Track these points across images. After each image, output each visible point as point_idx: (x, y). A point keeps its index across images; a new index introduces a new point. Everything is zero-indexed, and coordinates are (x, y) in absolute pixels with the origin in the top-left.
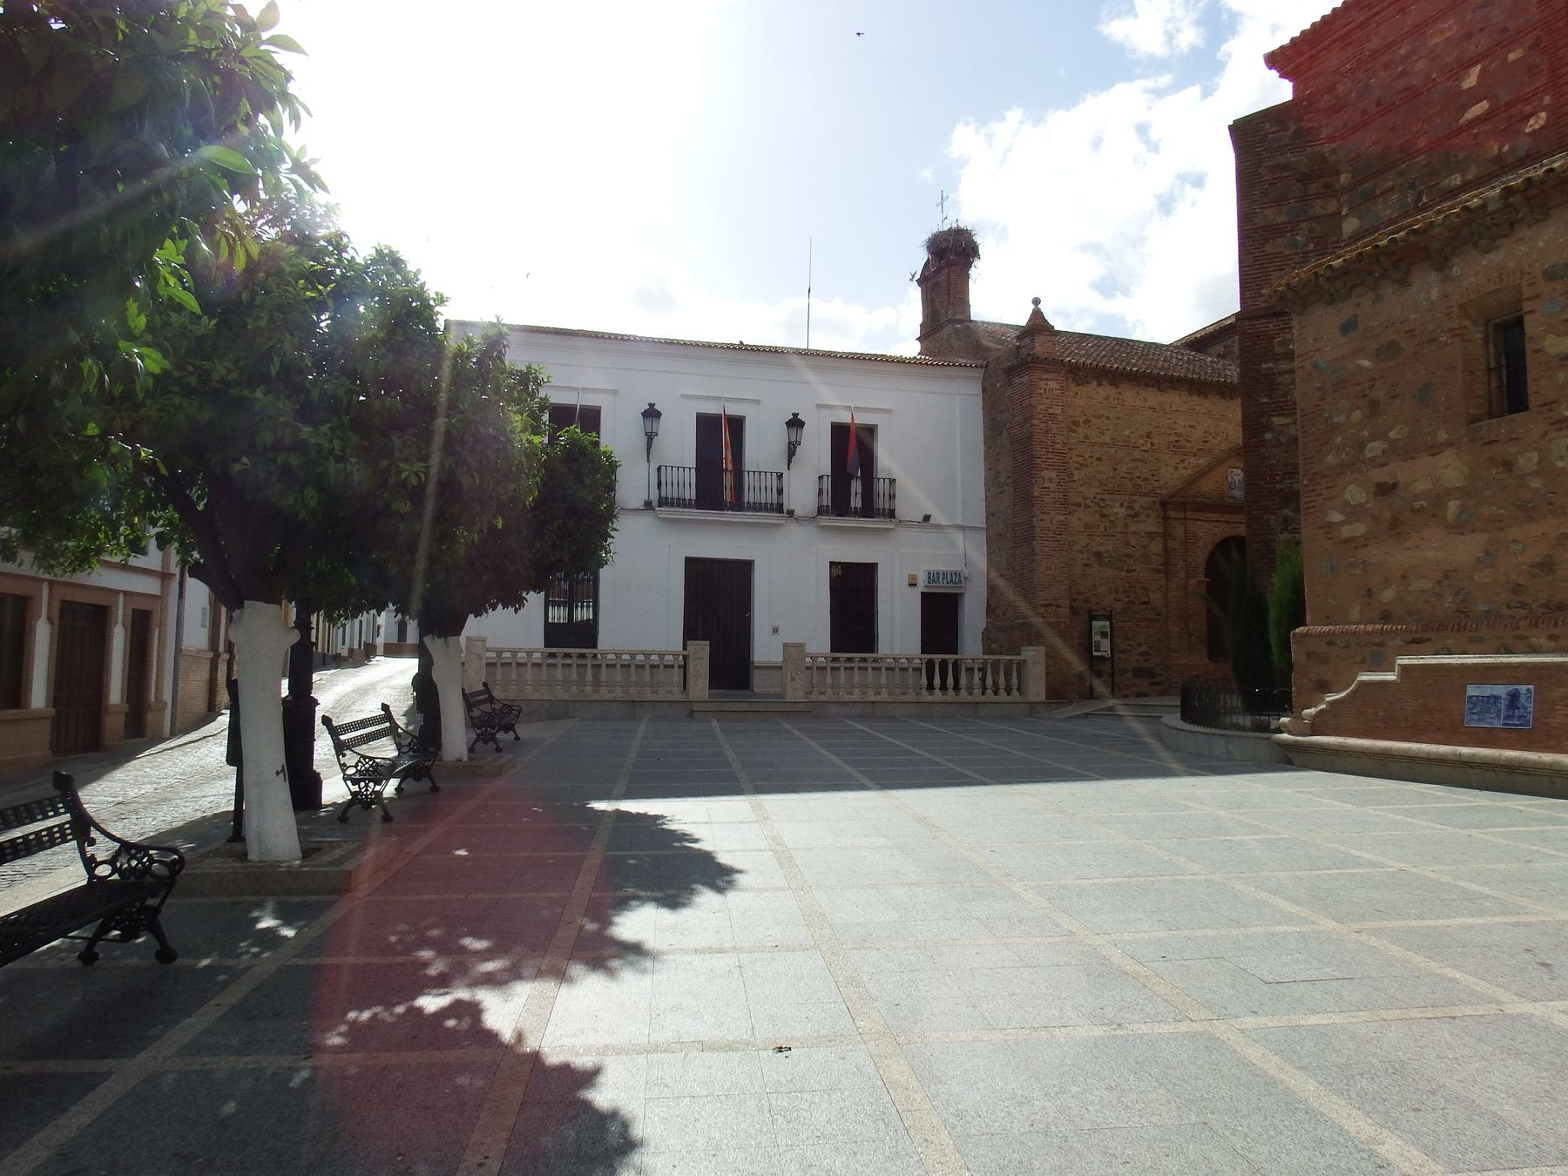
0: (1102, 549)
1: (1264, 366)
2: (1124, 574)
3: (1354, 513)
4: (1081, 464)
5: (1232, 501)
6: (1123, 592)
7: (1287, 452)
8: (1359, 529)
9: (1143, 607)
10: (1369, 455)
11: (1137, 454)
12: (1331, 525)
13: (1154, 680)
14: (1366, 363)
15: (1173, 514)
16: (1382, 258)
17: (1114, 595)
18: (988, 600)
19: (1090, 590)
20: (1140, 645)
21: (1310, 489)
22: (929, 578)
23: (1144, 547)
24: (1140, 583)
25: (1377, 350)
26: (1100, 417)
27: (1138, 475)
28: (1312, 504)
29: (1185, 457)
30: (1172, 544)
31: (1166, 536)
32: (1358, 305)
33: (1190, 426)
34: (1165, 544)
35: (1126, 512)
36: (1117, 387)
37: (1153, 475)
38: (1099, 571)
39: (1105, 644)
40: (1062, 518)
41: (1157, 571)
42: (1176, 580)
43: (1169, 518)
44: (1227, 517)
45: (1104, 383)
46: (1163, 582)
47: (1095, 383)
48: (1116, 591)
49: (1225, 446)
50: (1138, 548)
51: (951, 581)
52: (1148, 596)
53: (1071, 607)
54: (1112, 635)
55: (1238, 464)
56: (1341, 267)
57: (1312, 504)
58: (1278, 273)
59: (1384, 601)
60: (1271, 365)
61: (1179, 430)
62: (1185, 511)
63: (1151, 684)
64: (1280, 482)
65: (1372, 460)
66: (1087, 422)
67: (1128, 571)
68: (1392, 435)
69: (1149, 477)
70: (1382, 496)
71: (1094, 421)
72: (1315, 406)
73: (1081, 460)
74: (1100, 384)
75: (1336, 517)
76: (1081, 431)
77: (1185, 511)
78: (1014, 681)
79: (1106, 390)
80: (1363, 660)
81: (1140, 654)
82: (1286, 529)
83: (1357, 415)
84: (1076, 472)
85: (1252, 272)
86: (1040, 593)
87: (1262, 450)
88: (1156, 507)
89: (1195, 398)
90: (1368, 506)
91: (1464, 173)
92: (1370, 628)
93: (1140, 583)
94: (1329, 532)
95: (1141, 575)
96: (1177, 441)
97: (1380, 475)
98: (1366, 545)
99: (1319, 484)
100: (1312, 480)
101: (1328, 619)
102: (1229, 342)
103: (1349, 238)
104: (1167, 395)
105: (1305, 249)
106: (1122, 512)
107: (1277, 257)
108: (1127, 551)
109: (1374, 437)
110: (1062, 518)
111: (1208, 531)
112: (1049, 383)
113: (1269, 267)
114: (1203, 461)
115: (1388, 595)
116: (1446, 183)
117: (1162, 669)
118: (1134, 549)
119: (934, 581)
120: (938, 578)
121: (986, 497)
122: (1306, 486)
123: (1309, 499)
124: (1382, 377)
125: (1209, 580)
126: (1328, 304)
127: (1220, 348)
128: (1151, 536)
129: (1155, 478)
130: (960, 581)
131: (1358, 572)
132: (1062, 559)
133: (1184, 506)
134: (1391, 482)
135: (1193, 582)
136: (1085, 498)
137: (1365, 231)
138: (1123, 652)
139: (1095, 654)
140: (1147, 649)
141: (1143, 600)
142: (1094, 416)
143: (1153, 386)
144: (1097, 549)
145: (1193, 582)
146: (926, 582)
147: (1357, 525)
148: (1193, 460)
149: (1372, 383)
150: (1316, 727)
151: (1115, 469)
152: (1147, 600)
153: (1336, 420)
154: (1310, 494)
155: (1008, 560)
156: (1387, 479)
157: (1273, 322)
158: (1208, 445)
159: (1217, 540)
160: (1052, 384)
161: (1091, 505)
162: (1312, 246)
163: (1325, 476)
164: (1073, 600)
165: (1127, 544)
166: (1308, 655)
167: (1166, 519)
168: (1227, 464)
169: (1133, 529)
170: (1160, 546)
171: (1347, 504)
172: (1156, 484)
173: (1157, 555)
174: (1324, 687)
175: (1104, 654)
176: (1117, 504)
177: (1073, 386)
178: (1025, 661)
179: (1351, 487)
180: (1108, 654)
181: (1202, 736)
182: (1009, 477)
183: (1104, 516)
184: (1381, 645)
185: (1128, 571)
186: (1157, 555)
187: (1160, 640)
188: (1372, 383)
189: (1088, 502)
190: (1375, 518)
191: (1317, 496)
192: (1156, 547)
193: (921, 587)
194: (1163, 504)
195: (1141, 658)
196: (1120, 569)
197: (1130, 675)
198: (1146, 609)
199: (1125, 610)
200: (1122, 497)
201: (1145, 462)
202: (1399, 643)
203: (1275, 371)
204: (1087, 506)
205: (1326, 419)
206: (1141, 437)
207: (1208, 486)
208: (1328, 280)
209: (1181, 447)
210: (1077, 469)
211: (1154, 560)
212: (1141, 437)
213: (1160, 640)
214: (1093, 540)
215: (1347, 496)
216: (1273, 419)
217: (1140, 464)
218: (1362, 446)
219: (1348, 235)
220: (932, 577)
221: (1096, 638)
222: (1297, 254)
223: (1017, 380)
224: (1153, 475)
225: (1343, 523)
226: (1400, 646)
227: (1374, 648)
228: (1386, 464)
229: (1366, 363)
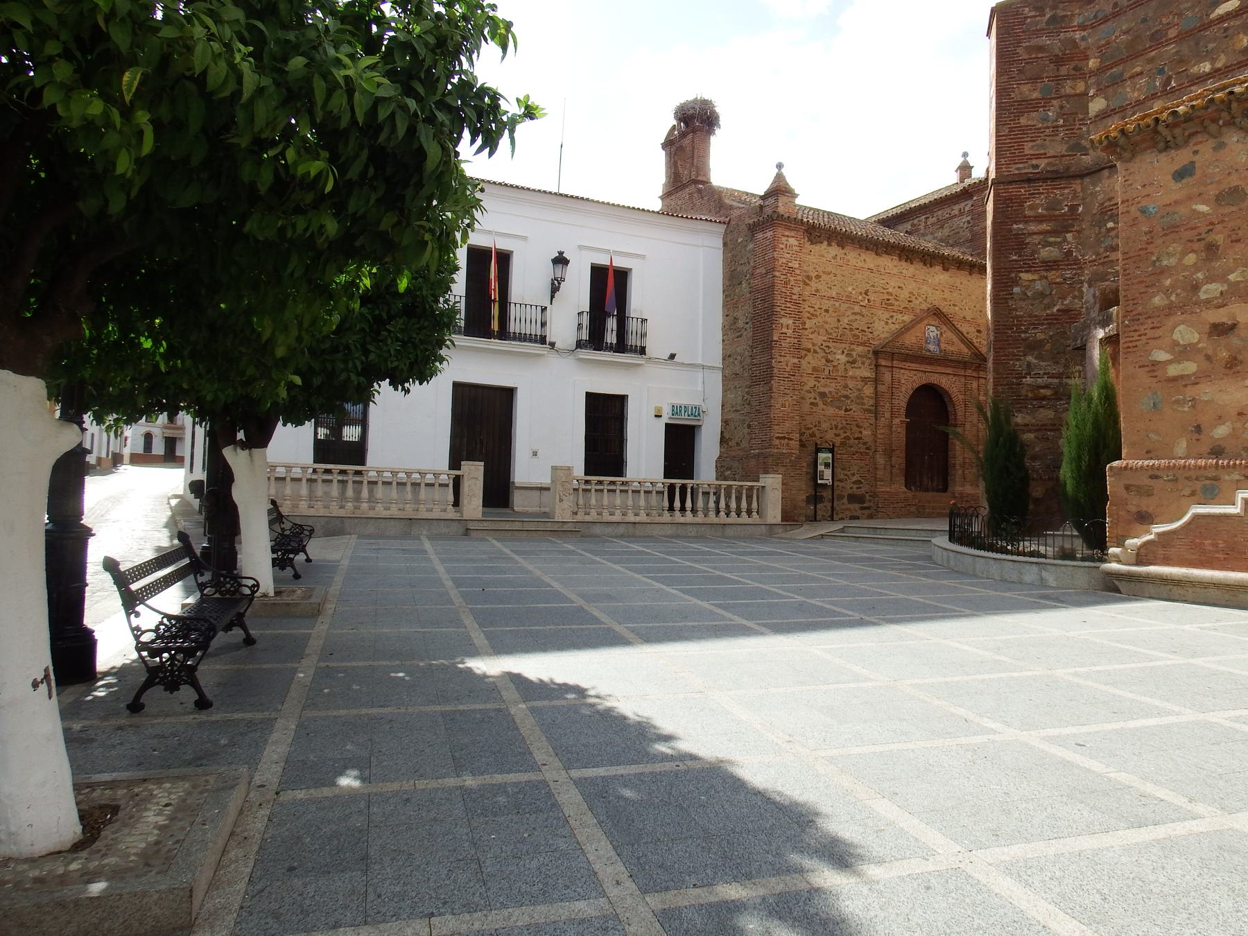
0: (826, 390)
2: (843, 412)
3: (1183, 352)
4: (812, 315)
5: (929, 354)
6: (842, 429)
7: (1032, 305)
8: (1190, 367)
9: (856, 441)
10: (1203, 296)
11: (857, 308)
12: (1155, 364)
13: (865, 505)
14: (1203, 208)
15: (883, 363)
16: (1234, 105)
17: (834, 431)
18: (722, 432)
19: (815, 426)
21: (1132, 329)
22: (673, 410)
23: (859, 390)
25: (1216, 196)
26: (829, 274)
28: (1134, 344)
29: (894, 314)
30: (881, 388)
31: (876, 381)
32: (1196, 152)
33: (899, 287)
34: (876, 387)
35: (847, 359)
36: (843, 248)
38: (823, 410)
39: (828, 473)
40: (796, 361)
41: (868, 411)
42: (883, 419)
43: (880, 365)
45: (833, 244)
46: (873, 421)
47: (825, 243)
48: (836, 427)
49: (925, 306)
51: (677, 413)
52: (861, 432)
53: (800, 440)
54: (832, 465)
55: (933, 323)
56: (1186, 113)
57: (1134, 344)
58: (1031, 144)
59: (1216, 436)
60: (1021, 226)
61: (890, 290)
63: (862, 509)
64: (1025, 332)
65: (1208, 301)
66: (818, 277)
67: (846, 410)
68: (1232, 277)
70: (1219, 336)
71: (824, 276)
72: (1140, 249)
73: (811, 310)
74: (829, 245)
75: (1162, 356)
76: (814, 285)
78: (755, 505)
79: (834, 250)
80: (1193, 494)
82: (1029, 374)
83: (1191, 259)
84: (807, 321)
85: (1008, 141)
86: (776, 427)
87: (1010, 303)
88: (870, 355)
89: (903, 263)
90: (1200, 345)
91: (1213, 61)
92: (1202, 462)
94: (1154, 371)
95: (855, 414)
96: (888, 300)
97: (1220, 316)
98: (1197, 384)
99: (1142, 324)
100: (1133, 320)
101: (1149, 454)
102: (916, 221)
103: (1096, 116)
104: (882, 259)
105: (1055, 124)
106: (843, 358)
107: (1031, 129)
108: (845, 393)
109: (1210, 279)
110: (796, 361)
111: (909, 379)
112: (790, 240)
113: (1023, 138)
114: (907, 318)
115: (1221, 431)
116: (1195, 70)
117: (870, 496)
118: (851, 391)
119: (677, 413)
120: (680, 411)
121: (723, 341)
122: (1127, 326)
123: (1132, 339)
124: (1222, 221)
126: (1160, 152)
127: (908, 226)
128: (864, 380)
129: (870, 330)
130: (699, 414)
131: (1186, 409)
132: (795, 397)
133: (892, 356)
134: (1230, 323)
135: (896, 421)
136: (814, 345)
137: (1112, 110)
138: (840, 481)
139: (819, 482)
141: (856, 436)
142: (824, 272)
143: (872, 250)
144: (822, 390)
145: (896, 421)
146: (670, 415)
147: (1187, 364)
148: (900, 316)
149: (1210, 227)
150: (1142, 557)
151: (839, 321)
153: (1165, 263)
154: (1132, 334)
155: (744, 397)
156: (1224, 320)
157: (1025, 187)
158: (912, 305)
159: (916, 386)
160: (792, 241)
161: (819, 350)
162: (1061, 122)
163: (1149, 317)
164: (802, 434)
165: (846, 386)
166: (1127, 488)
167: (877, 366)
168: (926, 322)
170: (872, 390)
171: (1176, 343)
172: (870, 336)
174: (1145, 519)
175: (826, 482)
176: (840, 352)
177: (808, 245)
178: (763, 487)
179: (1181, 327)
180: (829, 482)
181: (1010, 563)
182: (747, 323)
183: (828, 361)
184: (1216, 479)
185: (846, 410)
187: (869, 471)
188: (1210, 227)
189: (817, 348)
190: (1208, 358)
191: (1139, 336)
192: (868, 390)
193: (665, 419)
194: (876, 353)
195: (855, 486)
196: (840, 408)
197: (845, 500)
198: (859, 443)
199: (843, 444)
200: (844, 345)
201: (863, 316)
202: (1237, 477)
203: (1025, 232)
204: (815, 352)
205: (1155, 262)
206: (861, 293)
207: (910, 339)
208: (1167, 126)
209: (891, 305)
210: (808, 318)
211: (866, 402)
212: (861, 293)
213: (869, 471)
214: (819, 382)
215: (1176, 336)
216: (1021, 275)
217: (858, 317)
218: (1196, 288)
219: (1094, 114)
220: (676, 410)
221: (821, 468)
222: (1048, 127)
223: (760, 236)
225: (1170, 362)
226: (1238, 481)
227: (1208, 482)
228: (1225, 305)
229: (1203, 208)
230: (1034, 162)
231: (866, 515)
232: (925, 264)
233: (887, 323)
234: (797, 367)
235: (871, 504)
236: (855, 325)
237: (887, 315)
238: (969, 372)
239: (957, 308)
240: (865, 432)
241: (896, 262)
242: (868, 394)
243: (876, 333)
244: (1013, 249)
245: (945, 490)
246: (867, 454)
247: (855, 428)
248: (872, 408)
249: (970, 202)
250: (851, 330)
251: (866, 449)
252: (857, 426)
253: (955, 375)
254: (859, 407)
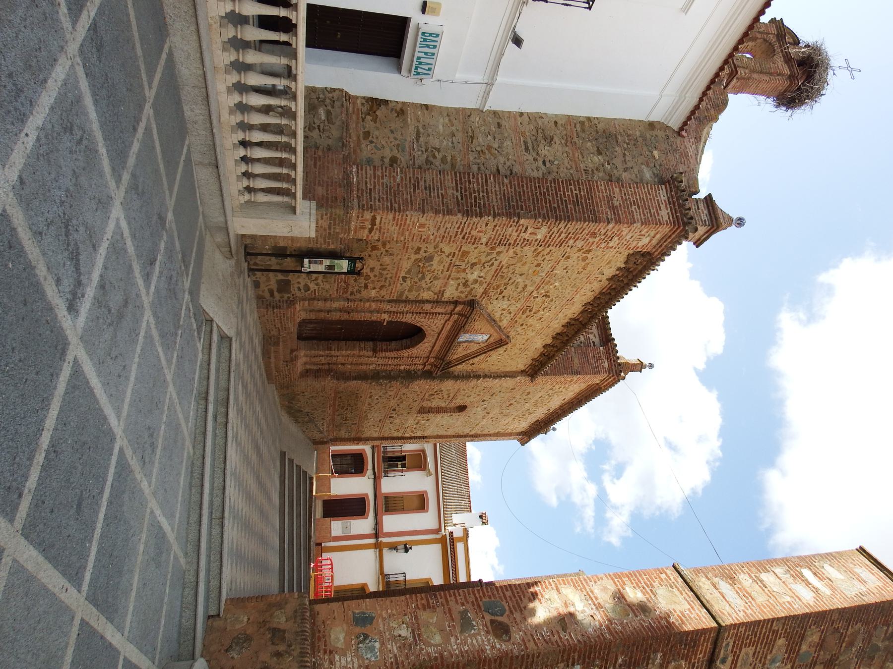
1: (659, 655)
2: (403, 274)
18: (386, 102)
19: (387, 251)
22: (431, 35)
27: (508, 289)
47: (623, 266)
58: (751, 653)
61: (541, 312)
74: (619, 269)
78: (262, 198)
85: (764, 630)
86: (391, 216)
88: (470, 298)
95: (399, 285)
107: (768, 650)
112: (648, 239)
113: (761, 644)
119: (425, 40)
120: (428, 46)
121: (521, 114)
125: (385, 324)
130: (418, 74)
146: (424, 29)
155: (439, 150)
157: (704, 657)
160: (646, 240)
161: (489, 258)
167: (456, 303)
178: (293, 210)
182: (544, 163)
183: (473, 265)
189: (494, 255)
193: (416, 18)
214: (448, 256)
220: (431, 39)
221: (327, 262)
223: (663, 195)
230: (730, 659)
232: (558, 334)
234: (475, 241)
241: (570, 315)
243: (495, 302)
244: (631, 658)
245: (300, 337)
247: (380, 284)
249: (597, 340)
254: (407, 288)
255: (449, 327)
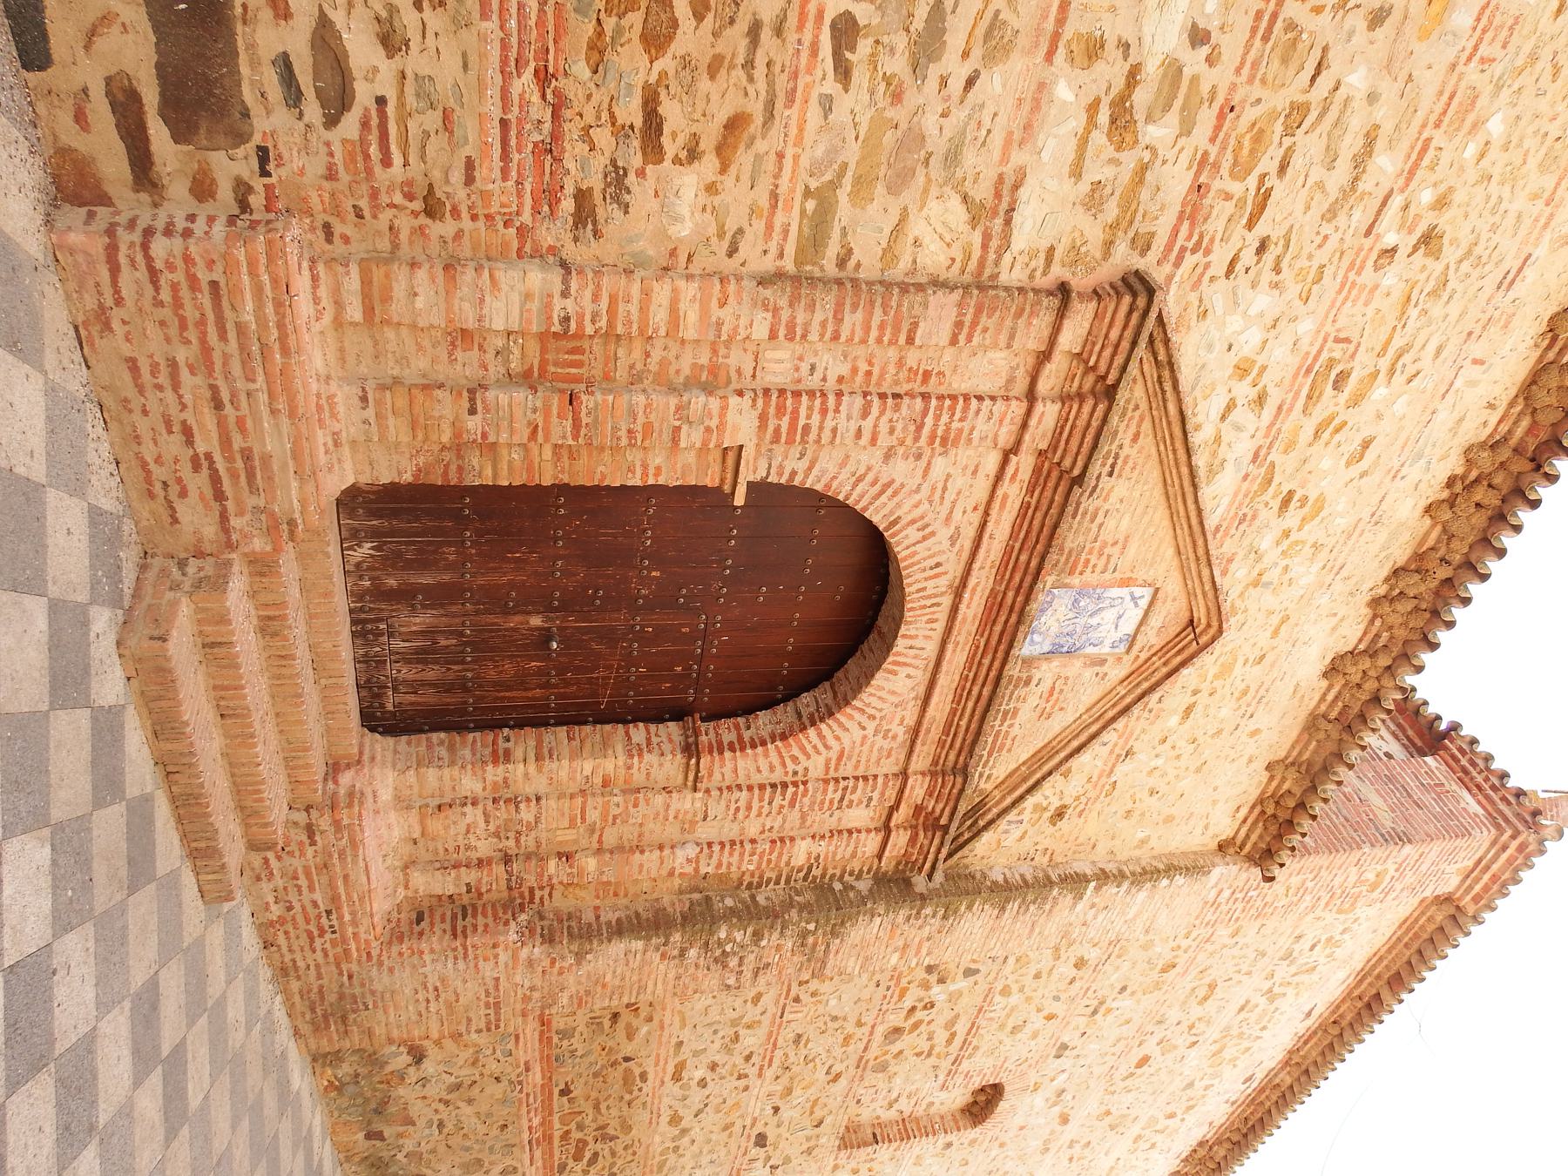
9: (631, 111)
13: (158, 132)
20: (391, 41)
23: (953, 157)
24: (770, 115)
27: (1297, 162)
33: (1366, 444)
34: (938, 284)
37: (1262, 248)
42: (761, 331)
44: (982, 581)
46: (755, 256)
50: (959, 115)
62: (1065, 399)
63: (126, 104)
69: (1262, 229)
77: (1065, 399)
81: (325, 38)
88: (1124, 257)
89: (1454, 464)
93: (770, 115)
95: (814, 114)
96: (1342, 378)
118: (956, 85)
125: (739, 500)
129: (1248, 257)
135: (742, 424)
140: (363, 94)
141: (670, 110)
145: (742, 424)
148: (1240, 448)
152: (670, 148)
168: (1173, 587)
169: (1063, 92)
170: (934, 257)
173: (898, 229)
186: (898, 229)
187: (432, 208)
194: (1138, 287)
195: (296, 40)
198: (621, 132)
200: (1231, 45)
211: (873, 209)
212: (1441, 203)
213: (432, 208)
224: (1262, 248)
231: (70, 135)
233: (1242, 370)
235: (178, 189)
236: (1309, 145)
237: (1281, 359)
238: (917, 790)
239: (1174, 721)
240: (689, 183)
242: (917, 228)
245: (376, 720)
246: (549, 196)
248: (833, 250)
250: (1297, 115)
251: (582, 196)
252: (735, 124)
253: (915, 732)
254: (852, 153)
255: (1025, 474)
